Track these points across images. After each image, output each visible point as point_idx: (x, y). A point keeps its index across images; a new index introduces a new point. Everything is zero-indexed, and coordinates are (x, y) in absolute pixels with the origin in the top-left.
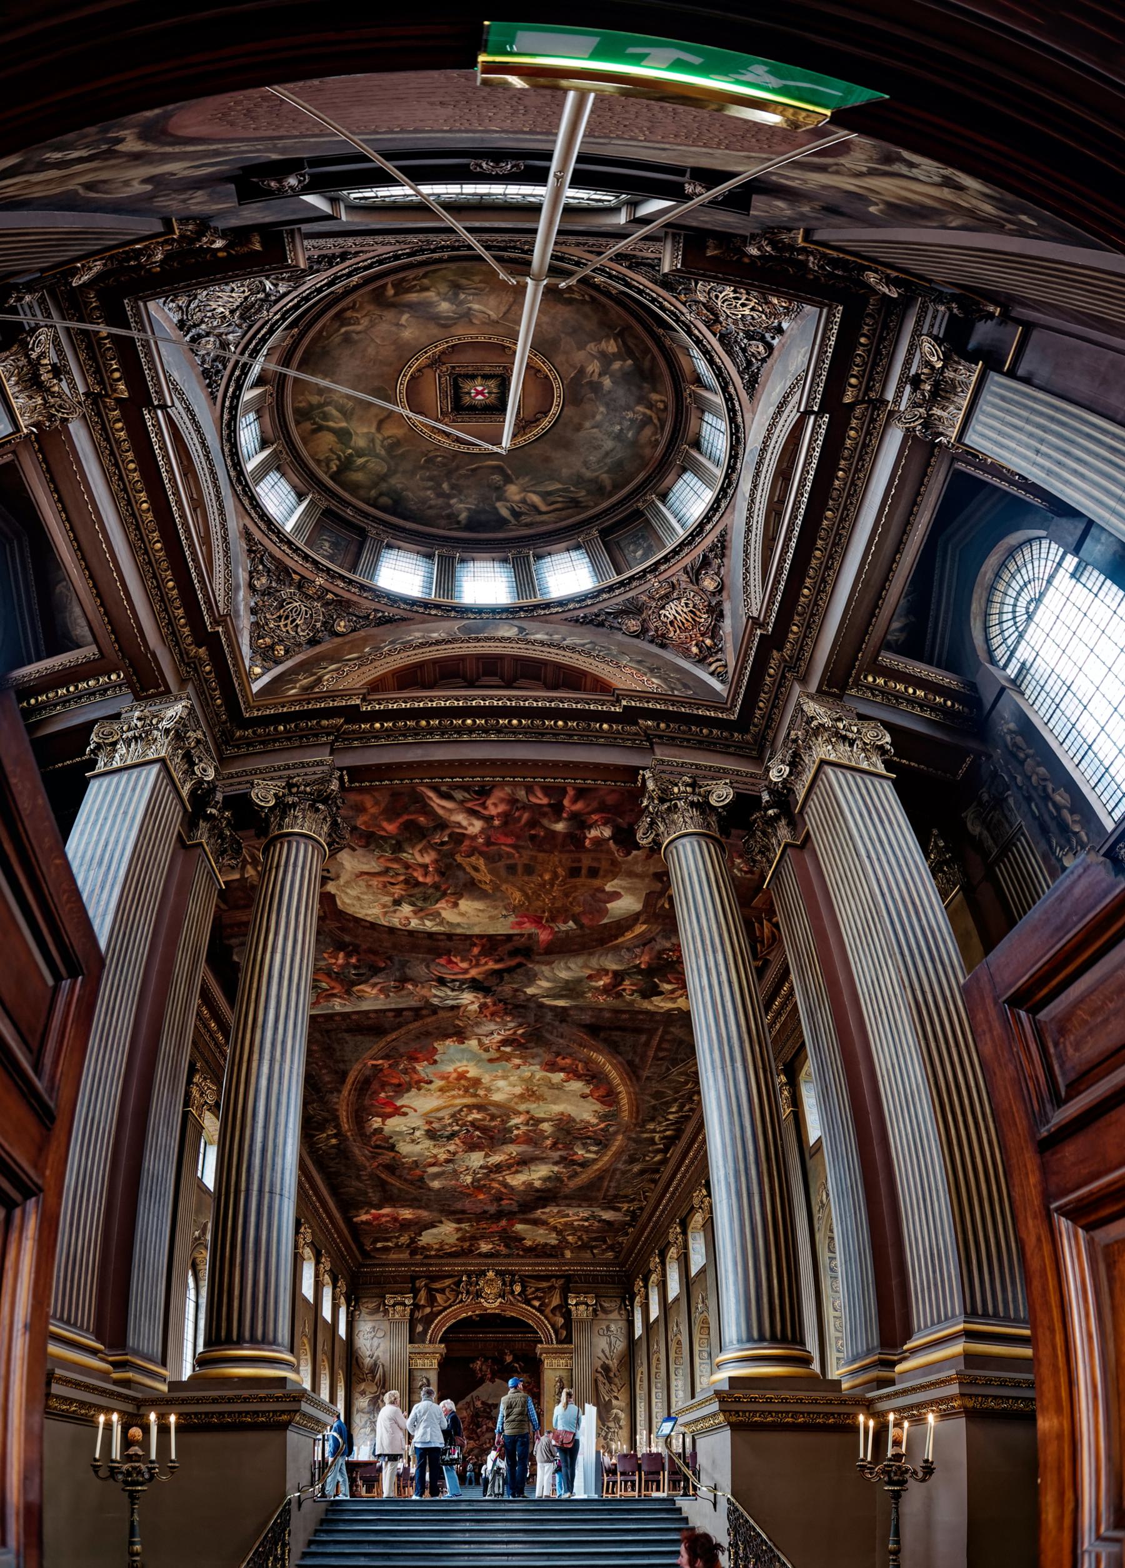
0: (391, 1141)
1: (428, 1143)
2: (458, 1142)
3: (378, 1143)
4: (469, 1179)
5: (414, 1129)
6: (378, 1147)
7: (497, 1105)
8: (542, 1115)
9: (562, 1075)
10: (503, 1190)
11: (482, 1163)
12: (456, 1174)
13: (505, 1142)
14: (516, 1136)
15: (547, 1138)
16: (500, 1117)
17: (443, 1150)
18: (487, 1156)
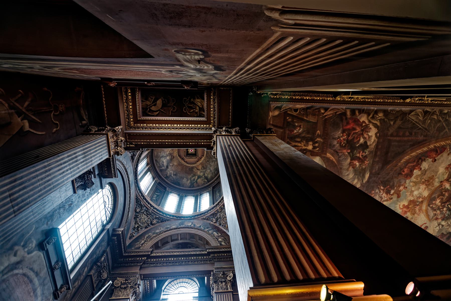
0: (445, 233)
5: (439, 225)
16: (442, 193)
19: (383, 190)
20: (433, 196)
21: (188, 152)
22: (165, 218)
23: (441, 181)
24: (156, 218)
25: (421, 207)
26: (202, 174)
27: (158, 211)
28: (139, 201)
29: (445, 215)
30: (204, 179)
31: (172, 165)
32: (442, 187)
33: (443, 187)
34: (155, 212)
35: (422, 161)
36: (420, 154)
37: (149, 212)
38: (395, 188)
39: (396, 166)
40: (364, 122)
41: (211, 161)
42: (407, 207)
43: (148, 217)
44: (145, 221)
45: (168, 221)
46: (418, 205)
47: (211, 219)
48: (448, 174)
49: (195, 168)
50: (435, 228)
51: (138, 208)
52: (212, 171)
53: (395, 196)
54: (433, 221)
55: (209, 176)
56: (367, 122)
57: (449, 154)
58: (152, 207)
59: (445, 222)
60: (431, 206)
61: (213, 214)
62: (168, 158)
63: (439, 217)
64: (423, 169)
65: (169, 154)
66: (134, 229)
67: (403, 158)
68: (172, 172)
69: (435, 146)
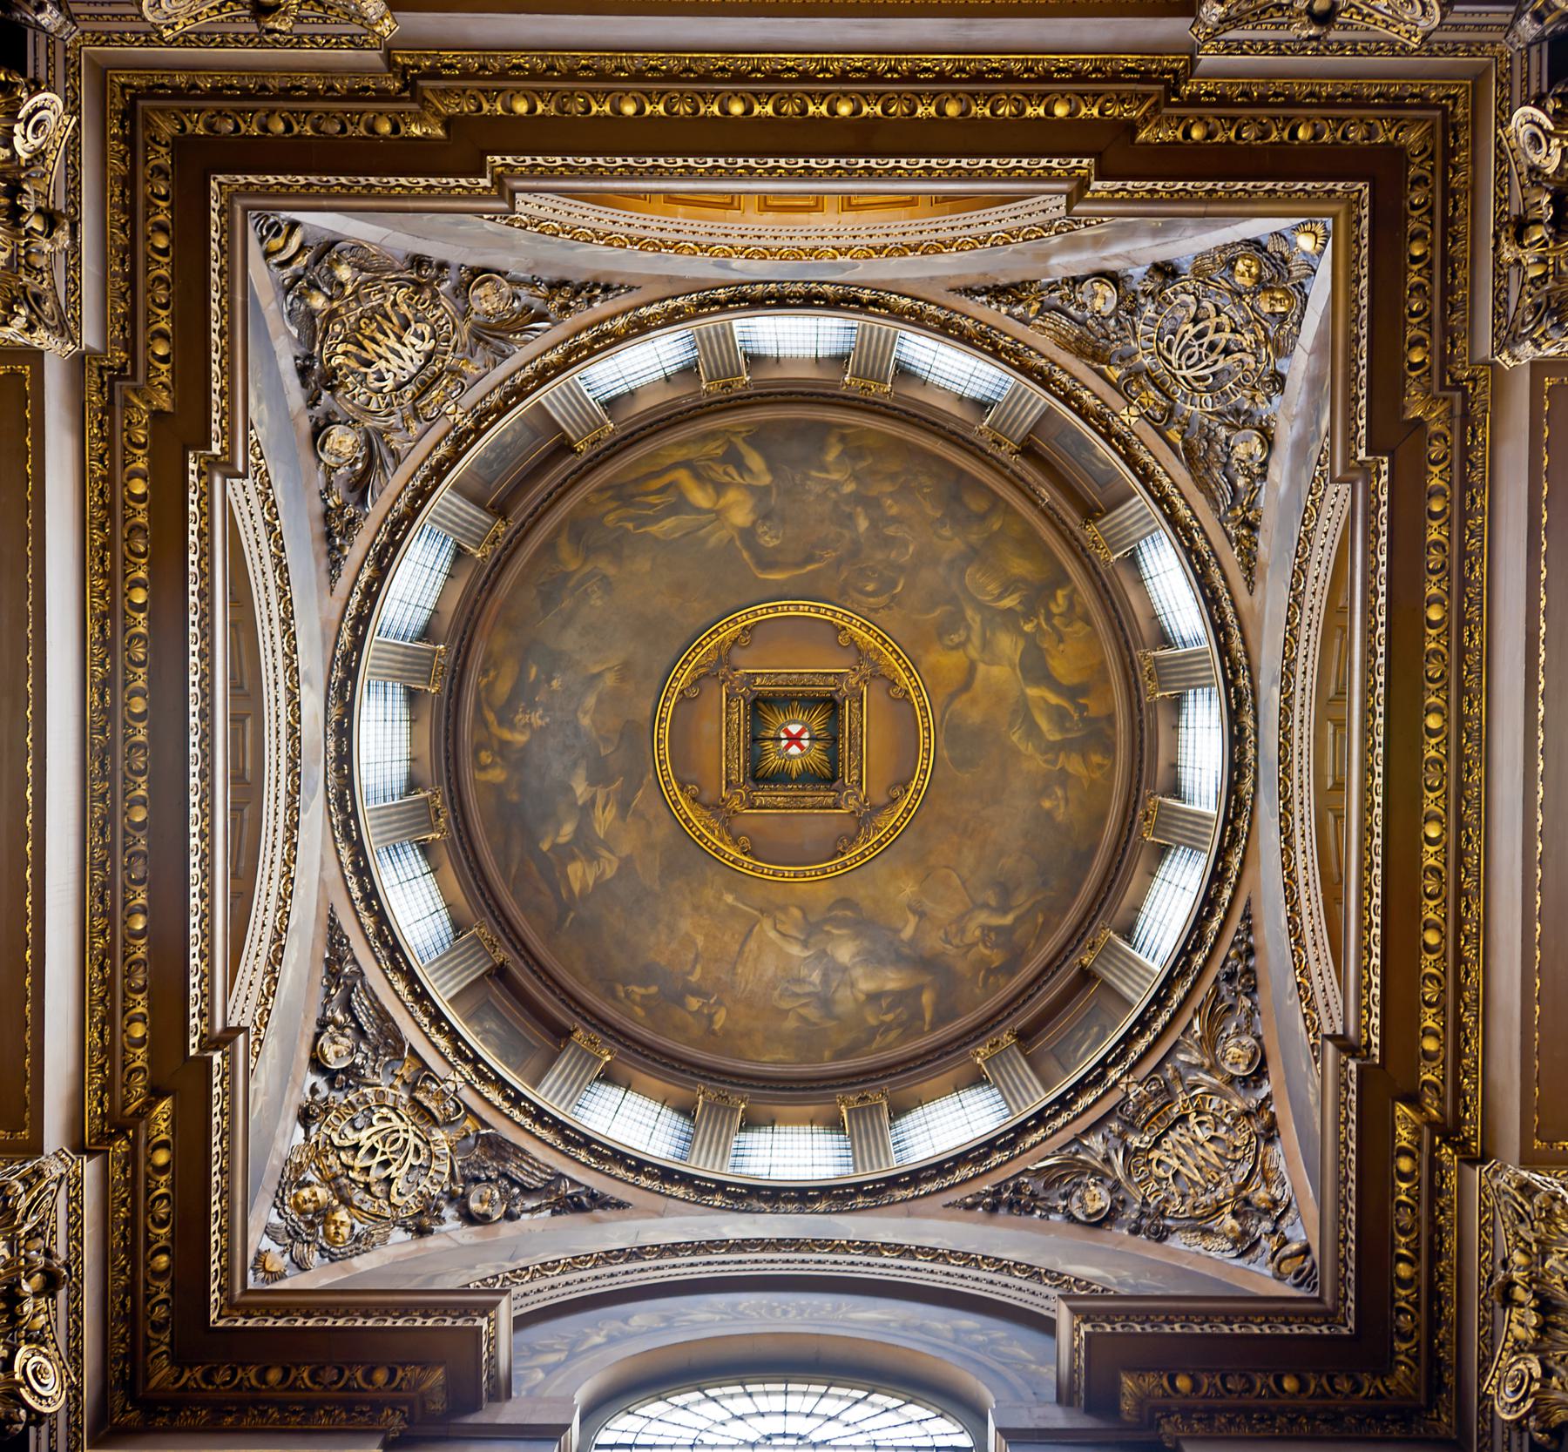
21: (809, 777)
22: (1227, 958)
24: (1210, 1042)
26: (1008, 645)
27: (1154, 1018)
28: (1017, 1190)
30: (1049, 616)
31: (913, 920)
34: (1150, 1048)
37: (1140, 1107)
41: (880, 556)
43: (1183, 1119)
44: (1212, 1139)
45: (1250, 930)
47: (1241, 482)
49: (957, 705)
51: (1081, 1199)
52: (973, 538)
55: (1020, 567)
58: (1103, 1076)
61: (1191, 458)
62: (844, 952)
65: (805, 944)
66: (1245, 1245)
68: (983, 917)
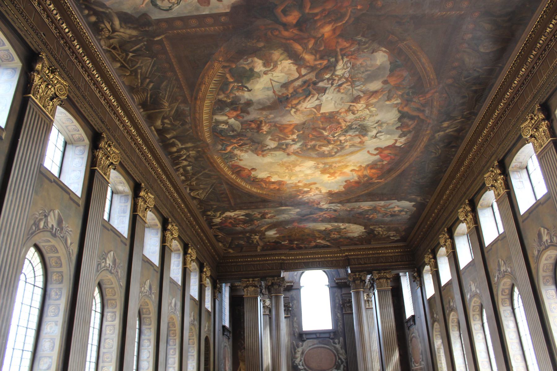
0: (399, 124)
1: (369, 122)
2: (343, 124)
3: (410, 123)
4: (341, 69)
5: (376, 137)
6: (412, 118)
7: (311, 158)
8: (278, 153)
9: (273, 180)
10: (298, 48)
11: (324, 98)
12: (352, 80)
13: (302, 126)
14: (293, 133)
15: (268, 133)
16: (309, 149)
17: (360, 113)
18: (318, 107)
19: (303, 196)
20: (314, 156)
23: (286, 156)
25: (333, 162)
29: (356, 135)
32: (297, 152)
33: (299, 150)
35: (257, 179)
36: (246, 183)
38: (300, 188)
39: (268, 194)
40: (221, 219)
42: (332, 174)
46: (331, 166)
48: (271, 152)
50: (380, 139)
53: (313, 187)
54: (364, 145)
56: (220, 218)
57: (241, 160)
59: (371, 131)
60: (333, 154)
63: (359, 140)
64: (269, 175)
67: (256, 193)
69: (232, 174)
